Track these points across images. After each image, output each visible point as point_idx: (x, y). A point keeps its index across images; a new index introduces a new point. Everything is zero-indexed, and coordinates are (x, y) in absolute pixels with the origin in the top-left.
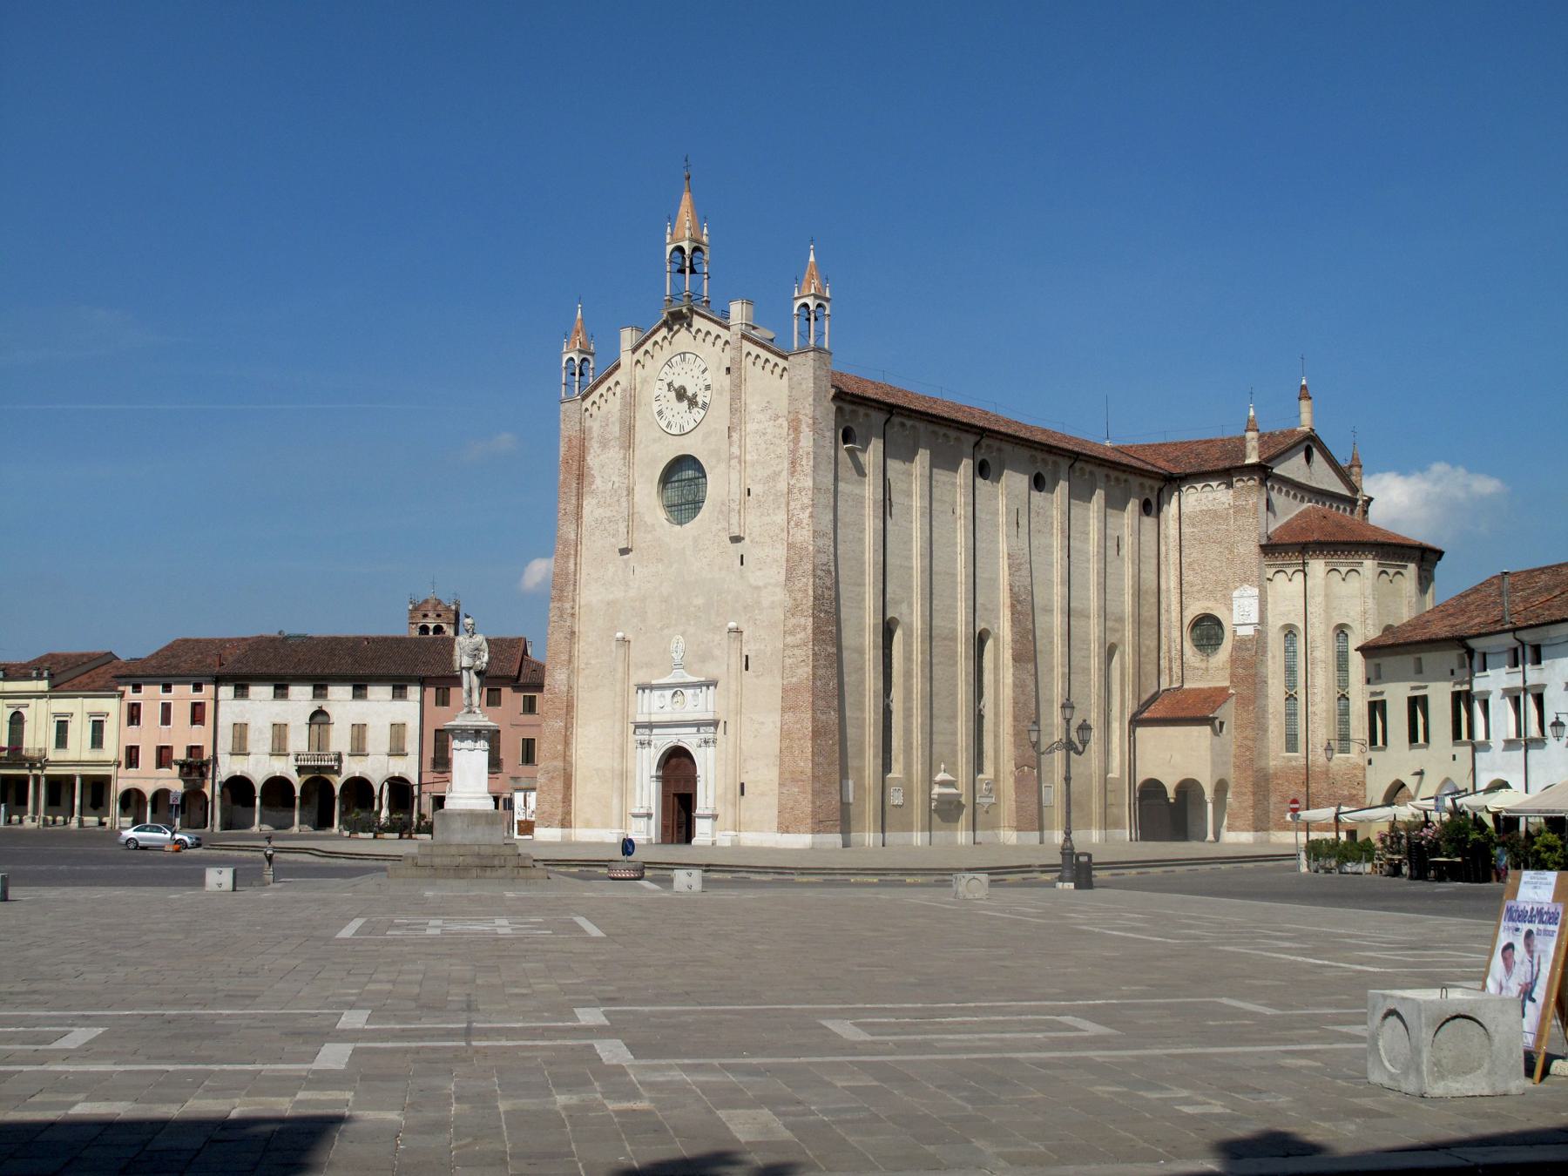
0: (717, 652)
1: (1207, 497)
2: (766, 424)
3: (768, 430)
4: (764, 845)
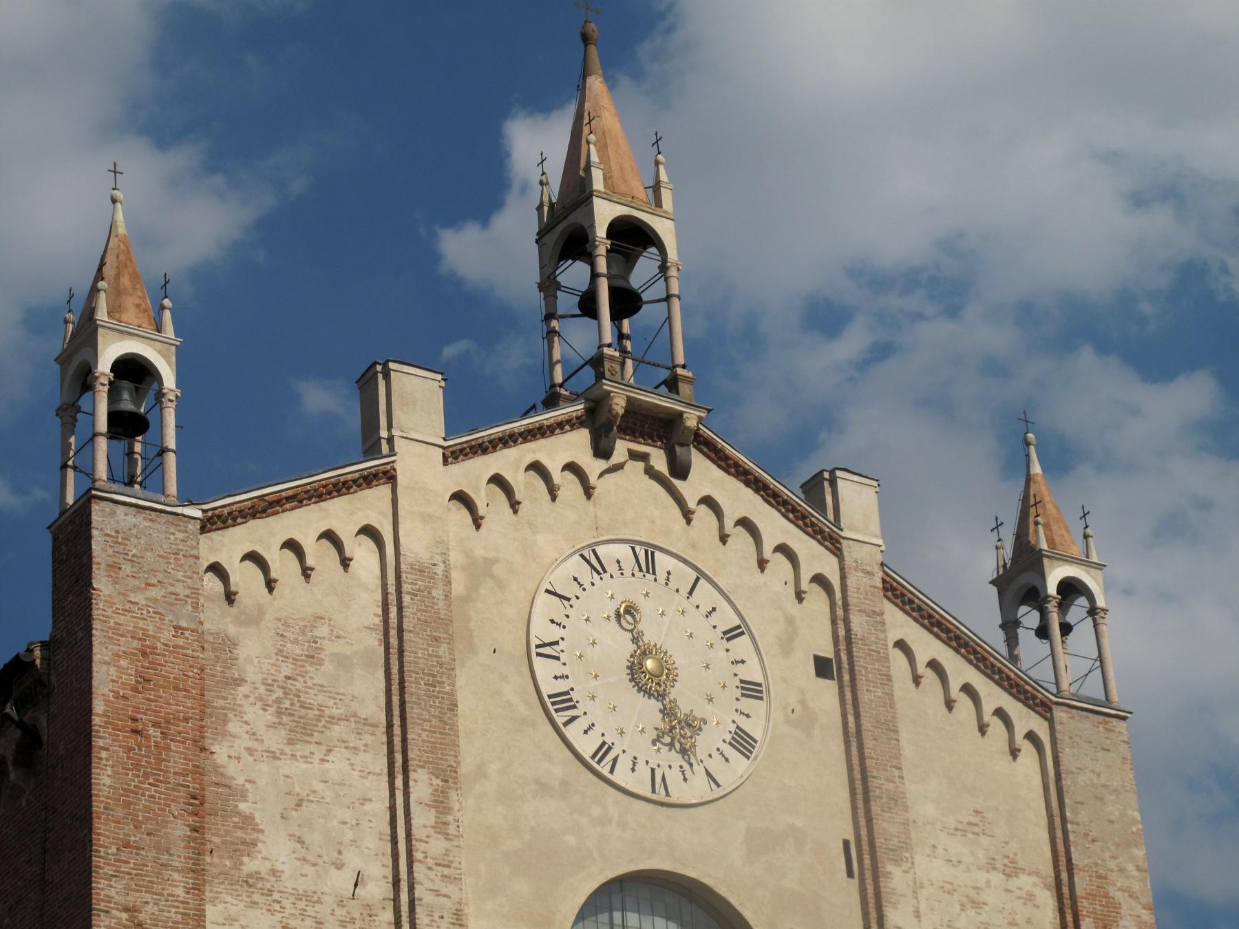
2: (982, 877)
3: (990, 898)
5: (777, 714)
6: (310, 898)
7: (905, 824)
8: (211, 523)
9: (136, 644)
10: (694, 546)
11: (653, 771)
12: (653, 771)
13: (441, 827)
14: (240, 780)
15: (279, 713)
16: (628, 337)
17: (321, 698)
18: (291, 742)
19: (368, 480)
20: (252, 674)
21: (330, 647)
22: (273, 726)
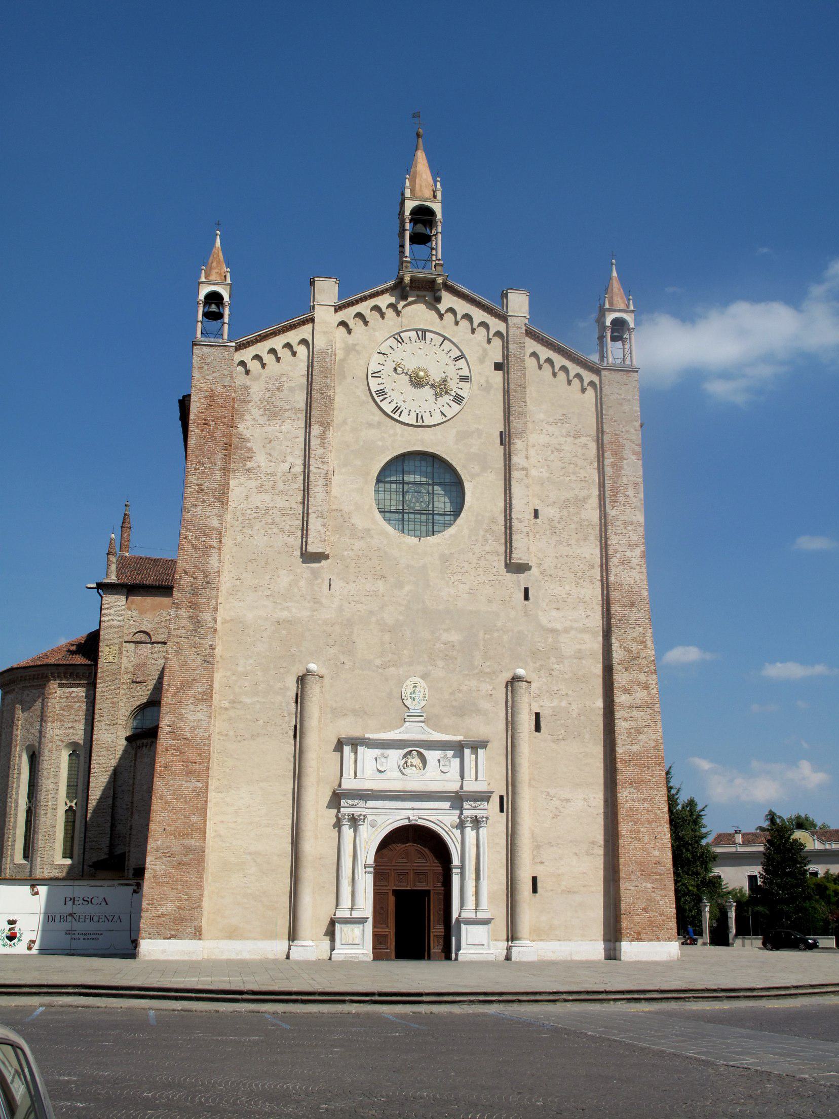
0: (485, 705)
2: (562, 440)
3: (566, 448)
4: (577, 958)
5: (475, 387)
6: (273, 474)
7: (525, 423)
8: (238, 348)
9: (207, 393)
10: (444, 327)
11: (417, 414)
12: (417, 414)
13: (322, 445)
14: (248, 436)
15: (265, 410)
17: (282, 403)
18: (269, 420)
19: (303, 323)
20: (255, 398)
21: (286, 385)
22: (262, 415)
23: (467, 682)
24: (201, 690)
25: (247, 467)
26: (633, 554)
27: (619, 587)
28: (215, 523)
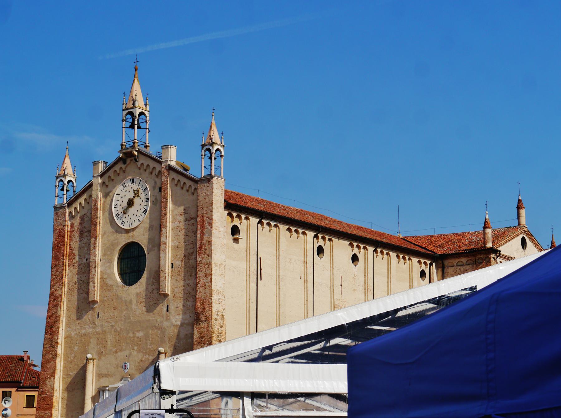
1: (460, 269)
16: (148, 129)
23: (145, 356)
24: (52, 371)
25: (73, 263)
26: (207, 281)
27: (200, 299)
28: (60, 293)
